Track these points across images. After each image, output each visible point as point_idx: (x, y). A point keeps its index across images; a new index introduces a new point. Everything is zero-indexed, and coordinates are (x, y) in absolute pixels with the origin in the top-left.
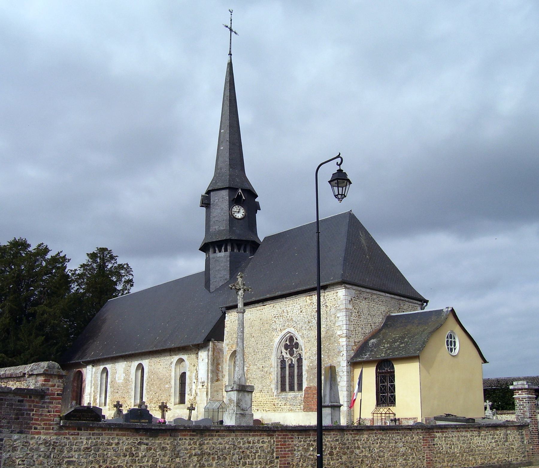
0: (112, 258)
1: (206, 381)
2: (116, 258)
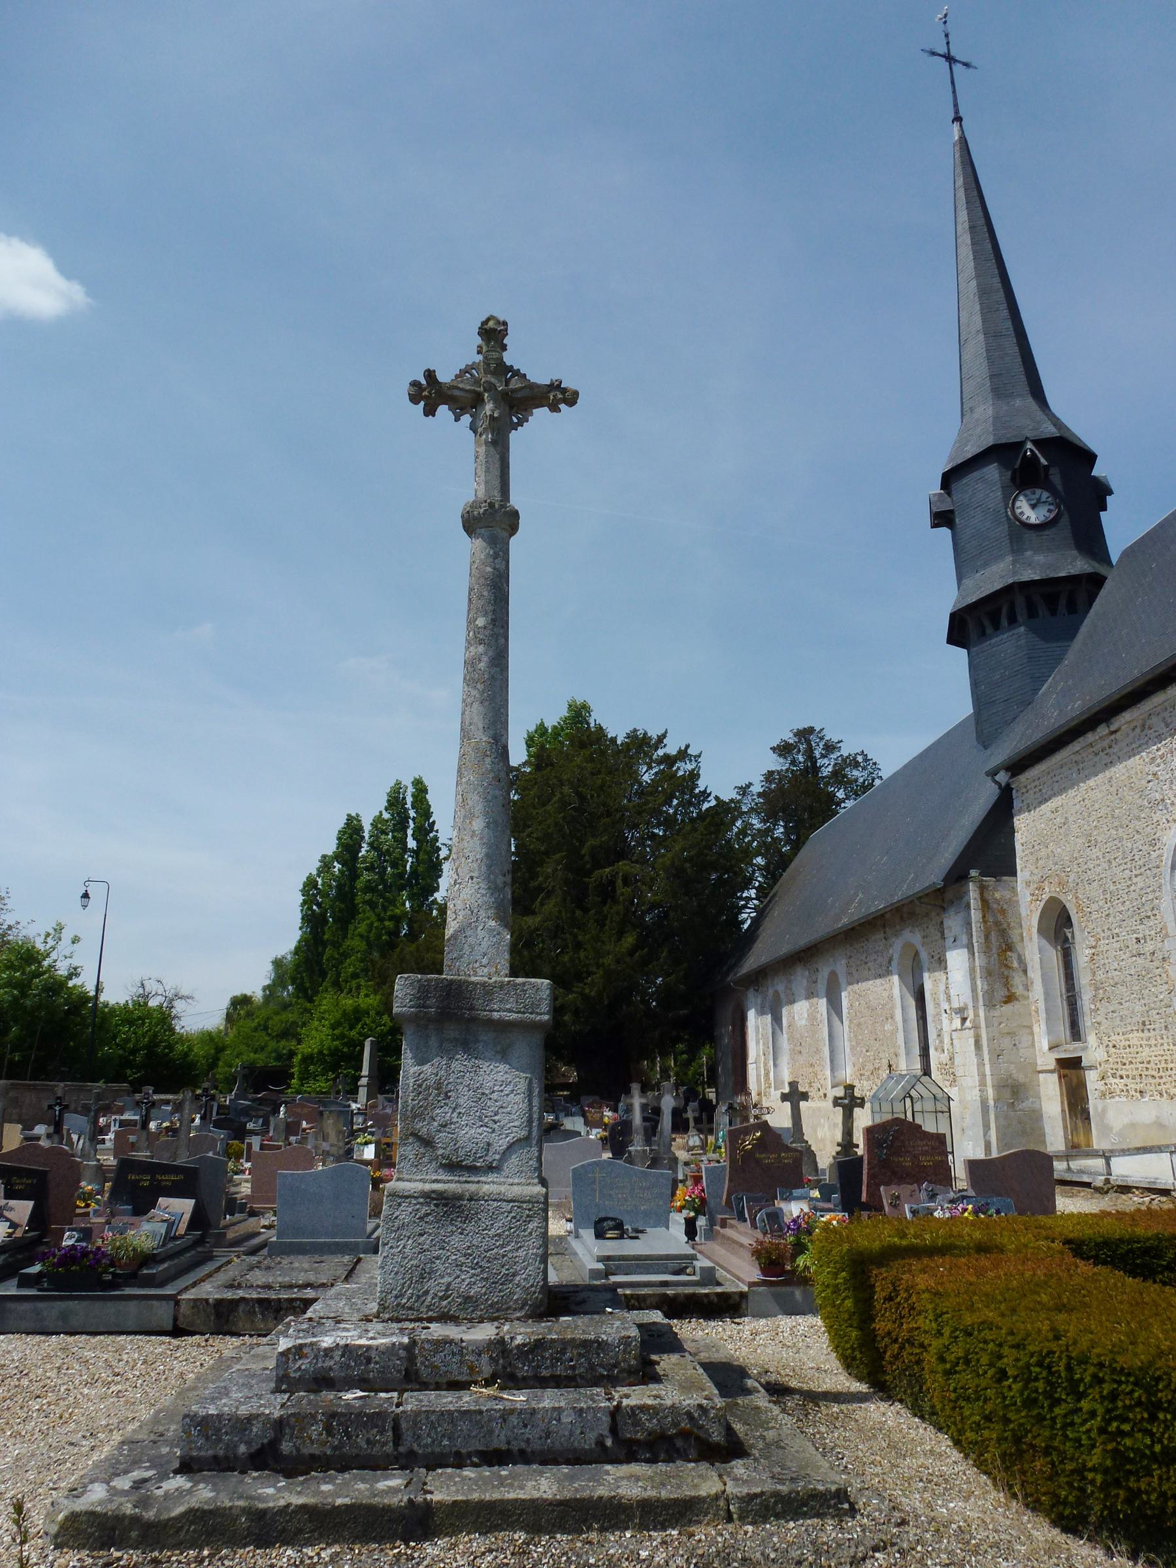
0: (830, 748)
1: (970, 1005)
2: (839, 745)
